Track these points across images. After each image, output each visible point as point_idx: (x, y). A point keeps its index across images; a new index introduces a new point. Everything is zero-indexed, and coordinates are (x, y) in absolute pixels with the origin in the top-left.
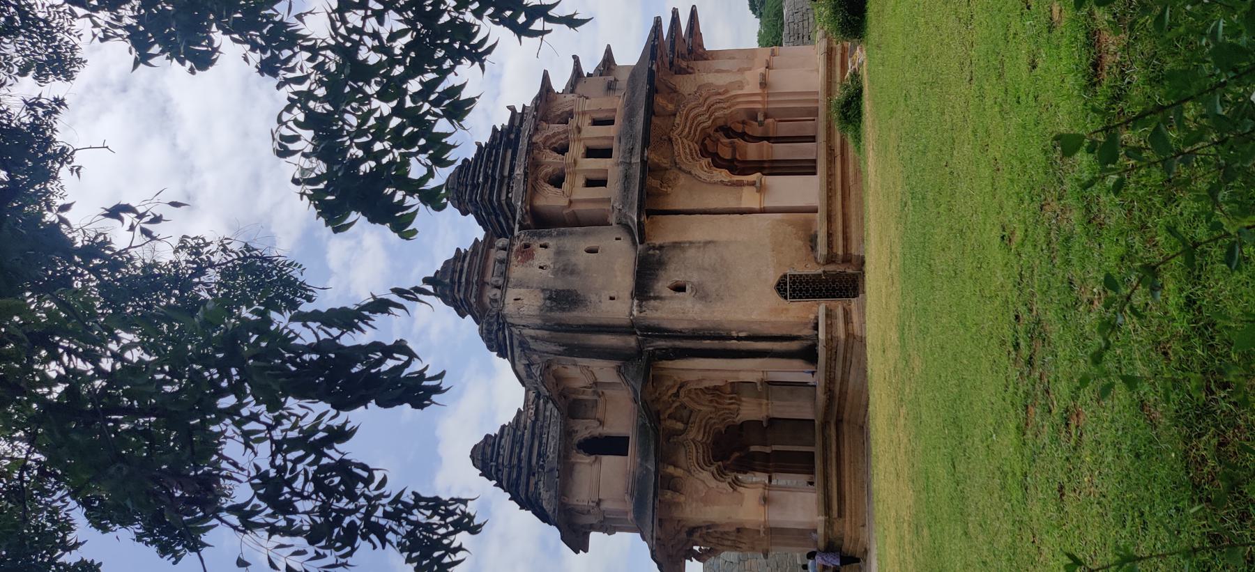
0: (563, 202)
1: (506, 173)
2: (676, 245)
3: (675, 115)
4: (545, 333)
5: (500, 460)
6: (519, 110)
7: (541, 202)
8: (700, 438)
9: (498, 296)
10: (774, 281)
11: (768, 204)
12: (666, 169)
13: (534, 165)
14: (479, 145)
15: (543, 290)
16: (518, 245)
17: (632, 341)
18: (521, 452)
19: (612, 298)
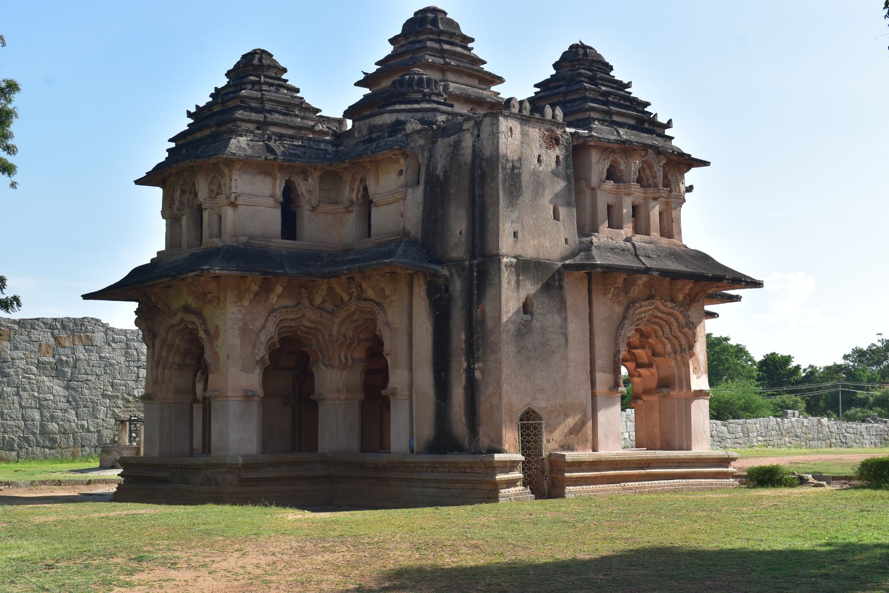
0: (594, 181)
1: (615, 118)
2: (563, 302)
3: (672, 301)
4: (469, 159)
5: (265, 88)
6: (668, 132)
7: (595, 156)
8: (306, 323)
12: (627, 293)
13: (626, 149)
14: (629, 85)
15: (520, 159)
17: (458, 250)
18: (279, 113)
19: (515, 234)
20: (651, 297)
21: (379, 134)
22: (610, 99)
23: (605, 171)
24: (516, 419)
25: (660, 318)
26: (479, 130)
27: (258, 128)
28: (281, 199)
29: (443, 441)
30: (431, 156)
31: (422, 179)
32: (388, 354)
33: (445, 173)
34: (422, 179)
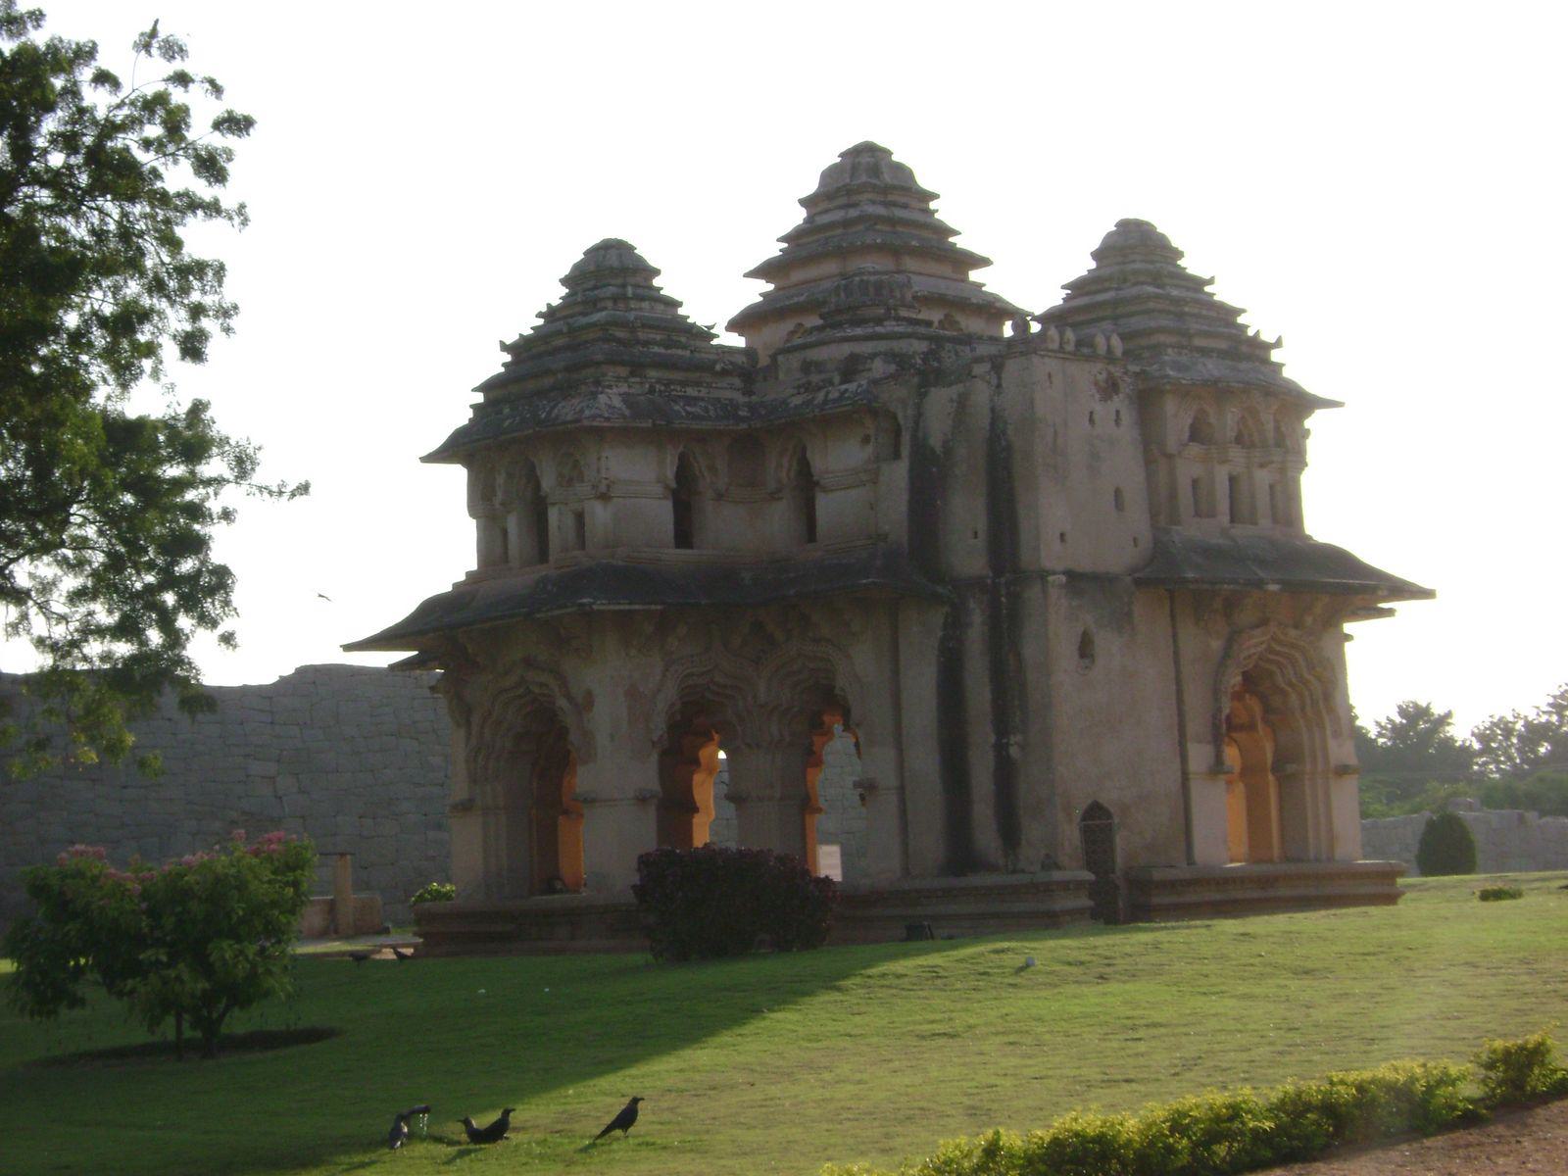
0: (1172, 444)
1: (1198, 342)
3: (1296, 627)
4: (986, 422)
5: (633, 304)
9: (1051, 346)
10: (1104, 799)
11: (1197, 789)
16: (1117, 371)
20: (1264, 622)
21: (823, 376)
22: (1187, 309)
23: (1187, 429)
24: (1079, 820)
25: (1278, 653)
26: (999, 378)
27: (632, 374)
28: (674, 485)
29: (961, 857)
30: (919, 415)
31: (905, 451)
32: (858, 725)
33: (945, 443)
34: (905, 451)
